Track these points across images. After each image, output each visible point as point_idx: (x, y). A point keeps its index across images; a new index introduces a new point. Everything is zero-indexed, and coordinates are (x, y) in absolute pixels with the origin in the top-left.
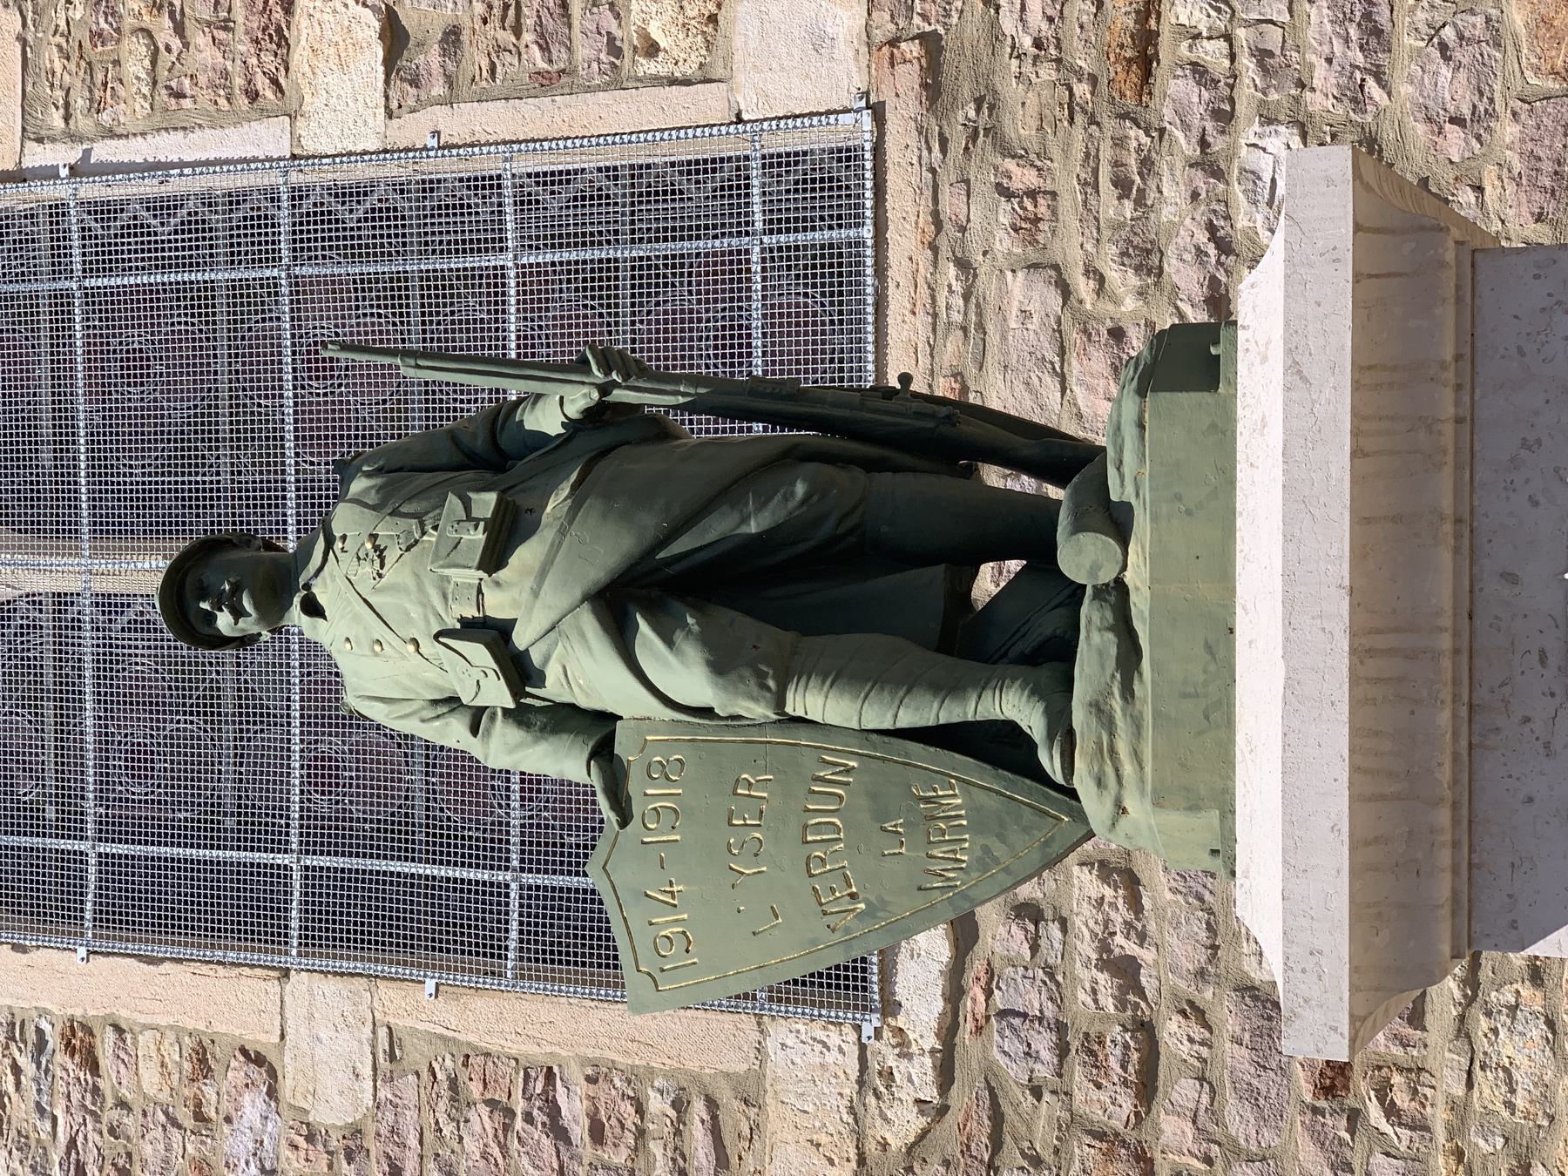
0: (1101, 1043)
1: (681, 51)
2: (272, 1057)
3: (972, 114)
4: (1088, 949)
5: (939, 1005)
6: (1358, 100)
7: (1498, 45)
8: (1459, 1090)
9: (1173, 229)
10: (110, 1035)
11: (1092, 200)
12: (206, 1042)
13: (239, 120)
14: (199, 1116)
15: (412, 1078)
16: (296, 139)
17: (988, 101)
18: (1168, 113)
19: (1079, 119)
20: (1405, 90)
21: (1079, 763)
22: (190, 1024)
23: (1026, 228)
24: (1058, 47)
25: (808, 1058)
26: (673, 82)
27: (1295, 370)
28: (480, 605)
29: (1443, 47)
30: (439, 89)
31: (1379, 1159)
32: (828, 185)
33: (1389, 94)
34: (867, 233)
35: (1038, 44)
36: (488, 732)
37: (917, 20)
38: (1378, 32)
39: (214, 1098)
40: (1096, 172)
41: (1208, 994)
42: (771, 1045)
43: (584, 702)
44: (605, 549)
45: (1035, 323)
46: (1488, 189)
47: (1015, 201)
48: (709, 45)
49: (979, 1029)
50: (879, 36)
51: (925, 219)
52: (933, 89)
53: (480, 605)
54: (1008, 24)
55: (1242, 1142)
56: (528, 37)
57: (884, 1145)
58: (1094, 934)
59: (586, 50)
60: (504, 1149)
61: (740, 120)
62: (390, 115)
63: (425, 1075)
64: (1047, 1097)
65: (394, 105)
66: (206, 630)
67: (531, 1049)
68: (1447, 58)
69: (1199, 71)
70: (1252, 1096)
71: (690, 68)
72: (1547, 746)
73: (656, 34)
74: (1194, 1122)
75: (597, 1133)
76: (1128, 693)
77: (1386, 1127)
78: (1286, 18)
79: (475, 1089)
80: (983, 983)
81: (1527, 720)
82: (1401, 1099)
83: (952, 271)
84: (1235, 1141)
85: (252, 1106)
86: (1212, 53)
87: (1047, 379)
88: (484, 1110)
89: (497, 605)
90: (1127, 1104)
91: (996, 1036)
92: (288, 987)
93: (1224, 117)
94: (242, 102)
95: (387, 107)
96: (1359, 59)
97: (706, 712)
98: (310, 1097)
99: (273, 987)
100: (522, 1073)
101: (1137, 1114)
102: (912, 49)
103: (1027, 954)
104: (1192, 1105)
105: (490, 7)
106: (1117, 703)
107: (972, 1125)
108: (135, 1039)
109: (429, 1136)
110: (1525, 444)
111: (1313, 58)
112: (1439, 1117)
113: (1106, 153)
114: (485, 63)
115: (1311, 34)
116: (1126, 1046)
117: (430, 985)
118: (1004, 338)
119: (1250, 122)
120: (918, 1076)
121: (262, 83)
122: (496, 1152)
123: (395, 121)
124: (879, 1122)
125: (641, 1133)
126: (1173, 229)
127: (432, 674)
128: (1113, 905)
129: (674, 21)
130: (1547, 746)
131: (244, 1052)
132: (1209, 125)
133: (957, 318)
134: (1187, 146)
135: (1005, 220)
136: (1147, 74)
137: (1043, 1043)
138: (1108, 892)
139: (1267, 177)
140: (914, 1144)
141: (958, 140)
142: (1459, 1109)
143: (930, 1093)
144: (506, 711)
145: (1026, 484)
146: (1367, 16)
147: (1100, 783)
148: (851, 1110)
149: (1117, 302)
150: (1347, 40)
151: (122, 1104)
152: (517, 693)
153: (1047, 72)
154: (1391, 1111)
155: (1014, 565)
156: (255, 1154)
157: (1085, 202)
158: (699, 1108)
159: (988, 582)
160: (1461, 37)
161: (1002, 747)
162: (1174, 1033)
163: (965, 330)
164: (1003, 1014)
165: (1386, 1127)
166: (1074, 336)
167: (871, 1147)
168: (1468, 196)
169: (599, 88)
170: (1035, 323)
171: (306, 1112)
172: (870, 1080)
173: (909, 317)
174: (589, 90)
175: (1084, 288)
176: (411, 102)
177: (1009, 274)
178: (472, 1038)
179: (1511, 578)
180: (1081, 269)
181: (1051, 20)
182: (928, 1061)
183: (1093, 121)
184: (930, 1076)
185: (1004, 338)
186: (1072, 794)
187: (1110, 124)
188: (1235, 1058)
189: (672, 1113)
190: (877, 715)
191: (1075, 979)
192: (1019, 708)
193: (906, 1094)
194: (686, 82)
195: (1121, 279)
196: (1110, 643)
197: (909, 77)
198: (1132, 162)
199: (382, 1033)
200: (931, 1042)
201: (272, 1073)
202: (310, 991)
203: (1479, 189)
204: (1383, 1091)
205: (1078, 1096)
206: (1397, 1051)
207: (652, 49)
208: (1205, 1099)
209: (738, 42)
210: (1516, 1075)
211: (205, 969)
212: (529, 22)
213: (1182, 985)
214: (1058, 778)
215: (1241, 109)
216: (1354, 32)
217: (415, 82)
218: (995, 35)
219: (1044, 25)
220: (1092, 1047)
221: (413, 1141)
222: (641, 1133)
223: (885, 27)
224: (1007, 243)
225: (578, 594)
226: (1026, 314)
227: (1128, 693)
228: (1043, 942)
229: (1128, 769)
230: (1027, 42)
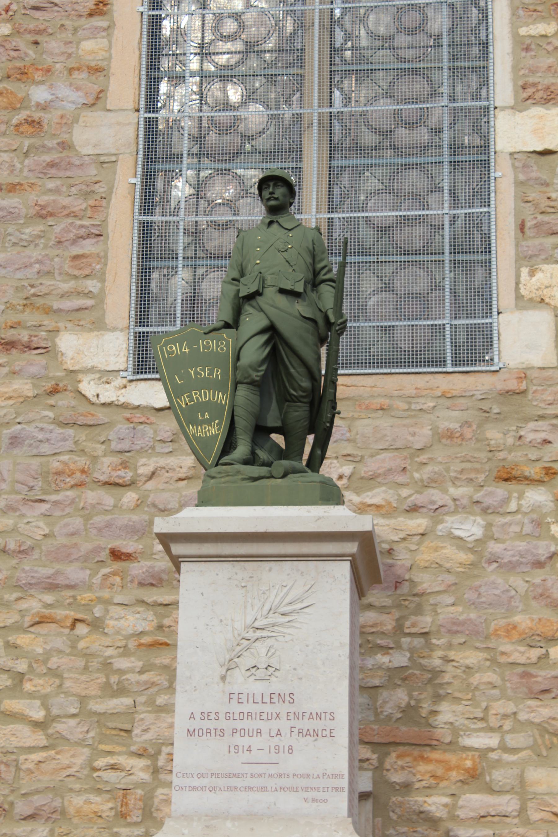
0: (125, 468)
1: (531, 284)
2: (100, 104)
3: (495, 411)
4: (162, 462)
5: (137, 403)
6: (490, 562)
7: (507, 610)
8: (116, 601)
9: (445, 491)
10: (105, 24)
11: (458, 461)
12: (105, 73)
13: (515, 81)
14: (71, 71)
15: (95, 172)
16: (503, 108)
17: (500, 418)
18: (490, 489)
19: (490, 455)
20: (493, 578)
21: (224, 467)
22: (113, 64)
23: (450, 435)
24: (520, 445)
25: (113, 348)
26: (517, 283)
27: (319, 518)
28: (270, 286)
29: (508, 591)
30: (522, 177)
31: (88, 572)
32: (474, 350)
33: (492, 572)
34: (451, 370)
35: (520, 437)
36: (232, 284)
37: (535, 388)
38: (514, 568)
39: (81, 77)
40: (469, 461)
41: (146, 509)
42: (118, 333)
43: (242, 317)
44: (286, 328)
45: (410, 438)
46: (453, 608)
47: (459, 429)
48: (531, 300)
49: (128, 419)
50: (528, 373)
51: (455, 393)
52: (509, 393)
53: (270, 286)
54: (532, 425)
55: (91, 522)
56: (540, 217)
57: (80, 381)
58: (167, 465)
59: (533, 243)
60: (68, 215)
61: (499, 313)
62: (511, 154)
63: (97, 179)
64: (103, 447)
65: (516, 156)
66: (264, 187)
67: (110, 228)
68: (503, 592)
69: (506, 501)
70: (108, 525)
71: (523, 291)
72: (230, 578)
73: (539, 275)
74: (98, 503)
75: (76, 258)
76: (243, 479)
77: (100, 575)
78: (524, 533)
79: (91, 202)
80: (146, 421)
81: (236, 574)
82: (112, 579)
83: (432, 404)
84: (91, 519)
85: (78, 97)
86: (513, 506)
87: (387, 444)
88: (83, 207)
89: (270, 293)
90: (103, 478)
91: (126, 426)
92: (131, 113)
93: (485, 511)
94: (521, 83)
95: (515, 152)
96: (506, 561)
97: (238, 359)
98: (84, 124)
99: (131, 105)
100: (99, 223)
101: (99, 482)
102: (523, 386)
103: (158, 438)
104: (103, 503)
105: (555, 200)
106: (240, 477)
107: (90, 417)
108: (103, 37)
109: (71, 181)
110: (302, 573)
111: (508, 543)
112: (106, 594)
113: (477, 466)
114: (530, 199)
115: (517, 543)
116: (124, 477)
117: (133, 181)
118: (404, 426)
119: (484, 520)
120: (109, 394)
121: (530, 91)
122: (66, 212)
123: (508, 157)
124: (89, 379)
125: (76, 277)
126: (445, 491)
127: (249, 268)
128: (179, 472)
129: (542, 284)
130: (230, 578)
131: (101, 91)
132: (484, 505)
133: (413, 407)
134: (477, 496)
135: (452, 426)
136: (506, 480)
137: (125, 445)
138: (184, 470)
139: (463, 527)
140: (81, 393)
141: (485, 406)
142: (108, 602)
143: (102, 400)
144: (238, 291)
145: (308, 449)
146: (522, 563)
147: (220, 473)
148: (93, 367)
149: (417, 471)
150: (513, 556)
151: (75, 30)
152: (244, 298)
153: (510, 441)
154: (106, 577)
155: (283, 446)
156: (57, 98)
157: (456, 457)
158: (89, 302)
159: (278, 439)
160: (512, 597)
161: (229, 446)
162: (130, 497)
163: (407, 410)
164: (134, 428)
165: (100, 575)
166: (405, 453)
167: (80, 376)
168: (450, 600)
169: (517, 250)
170: (410, 438)
171: (77, 122)
172: (106, 376)
173: (414, 387)
174: (517, 245)
175: (423, 458)
176: (517, 164)
177: (430, 427)
178: (113, 201)
179: (270, 570)
180: (430, 456)
181: (530, 442)
182: (114, 399)
183: (489, 459)
184: (108, 400)
185: (404, 426)
186: (217, 465)
187: (487, 467)
188: (123, 519)
189: (86, 291)
190: (239, 411)
191: (149, 458)
192: (242, 450)
193: (100, 389)
194: (517, 288)
195: (426, 473)
196: (256, 475)
197: (513, 385)
198: (473, 476)
199: (113, 158)
200: (122, 400)
201: (93, 105)
202: (129, 124)
203: (453, 605)
204: (114, 574)
205: (105, 460)
206: (129, 578)
207: (532, 274)
208: (106, 508)
209: (531, 312)
210: (122, 621)
211: (137, 72)
212: (546, 218)
213: (150, 499)
214: (221, 462)
215: (490, 517)
216: (514, 559)
217: (524, 166)
218: (527, 420)
219: (528, 440)
220: (124, 465)
221: (68, 174)
222: (76, 277)
223: (534, 374)
224: (443, 426)
225: (273, 319)
226: (414, 435)
227: (243, 479)
228: (164, 445)
229: (223, 480)
230: (522, 433)
